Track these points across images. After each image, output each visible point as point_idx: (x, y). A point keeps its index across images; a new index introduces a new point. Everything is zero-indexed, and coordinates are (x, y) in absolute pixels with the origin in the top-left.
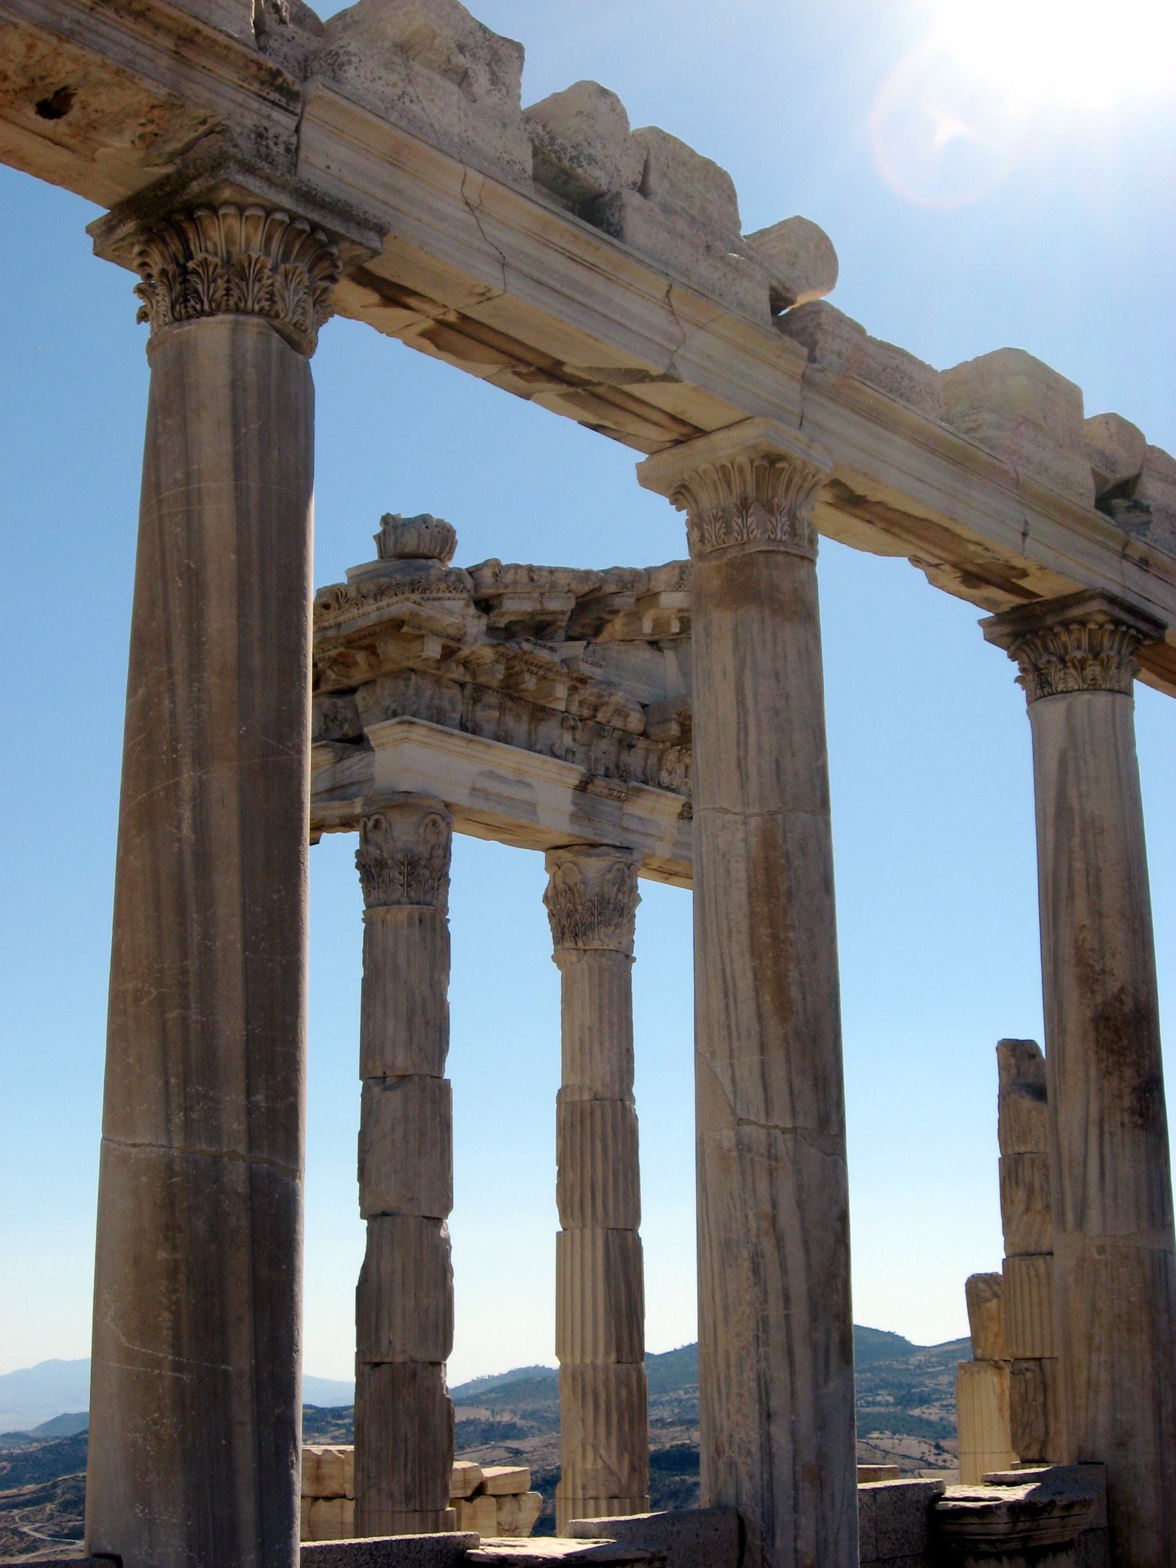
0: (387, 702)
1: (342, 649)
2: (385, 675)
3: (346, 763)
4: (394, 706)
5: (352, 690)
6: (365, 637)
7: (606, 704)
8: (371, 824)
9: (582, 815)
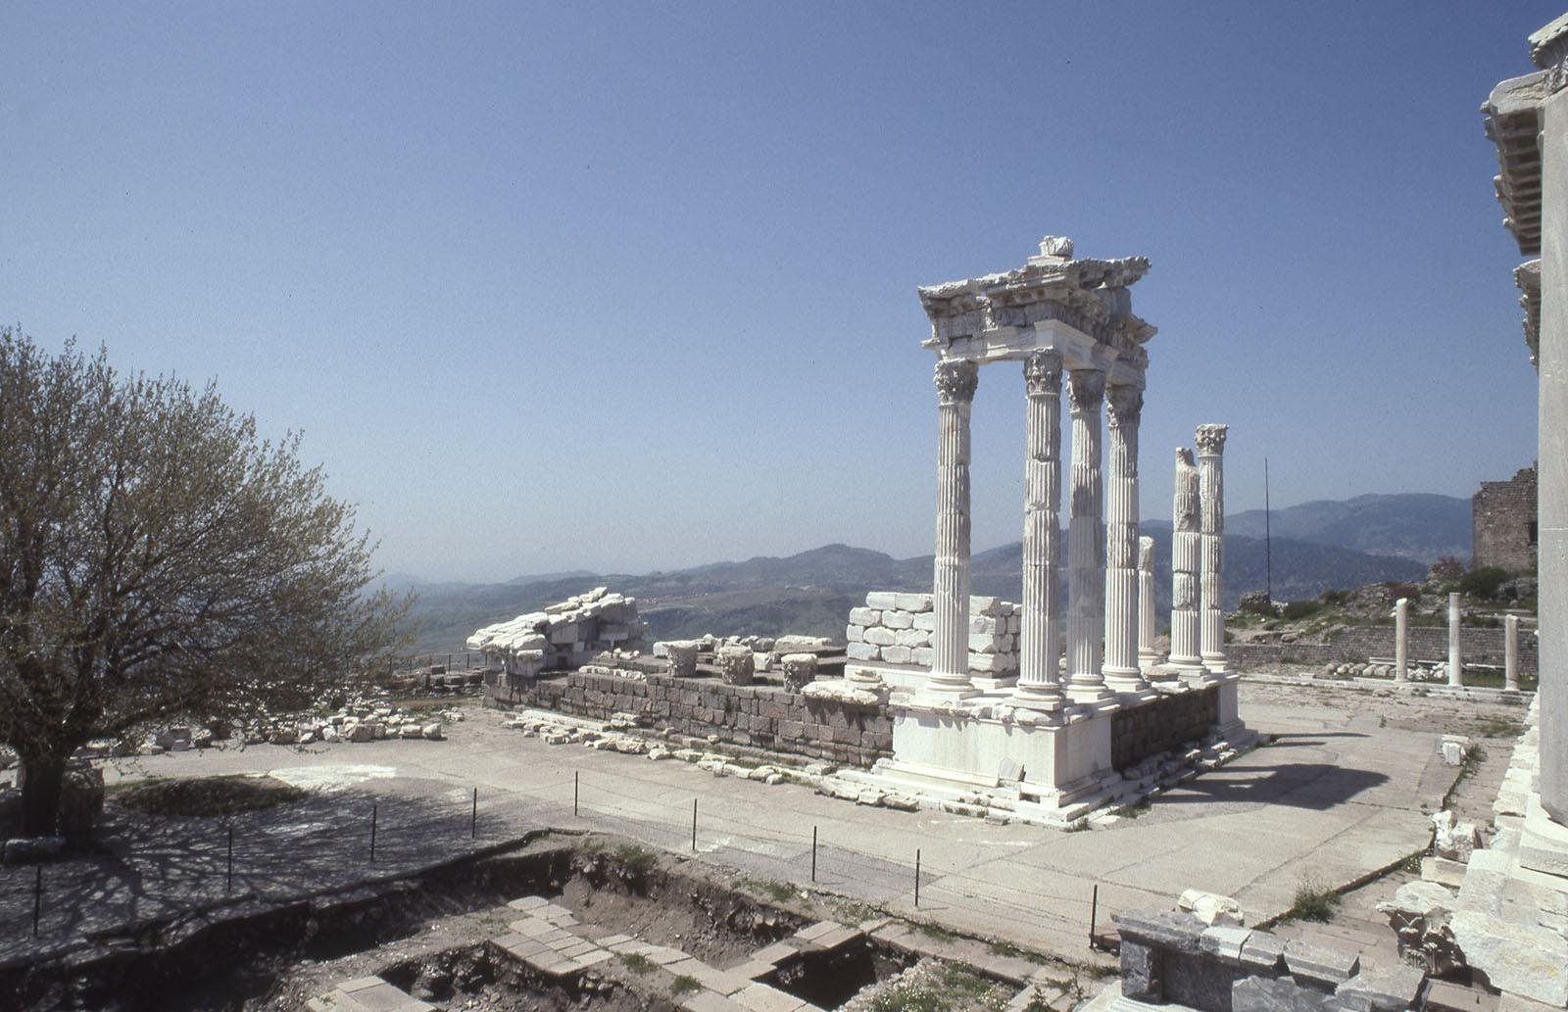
2: (1041, 301)
5: (1023, 306)
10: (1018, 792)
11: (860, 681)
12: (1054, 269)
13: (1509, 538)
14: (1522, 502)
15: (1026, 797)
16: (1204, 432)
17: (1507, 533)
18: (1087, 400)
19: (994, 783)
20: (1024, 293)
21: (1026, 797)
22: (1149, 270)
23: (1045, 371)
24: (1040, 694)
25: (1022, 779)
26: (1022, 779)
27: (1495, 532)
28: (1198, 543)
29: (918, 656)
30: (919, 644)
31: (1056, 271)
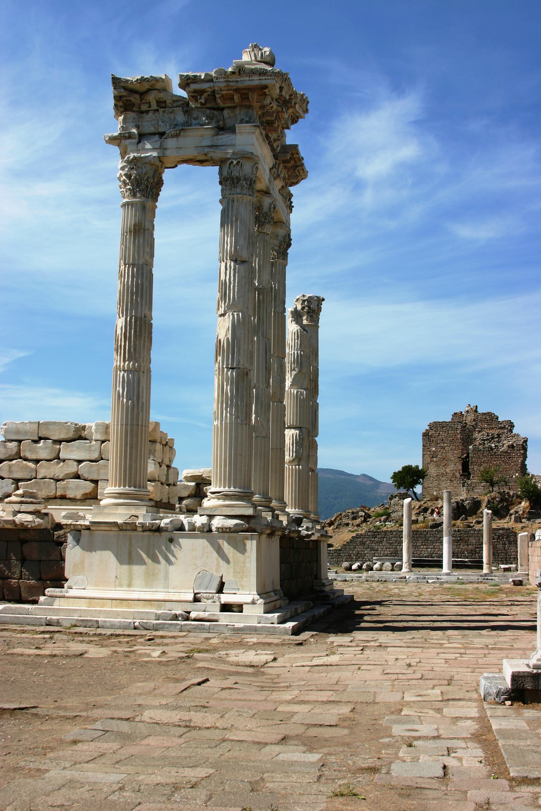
0: (243, 117)
1: (231, 92)
3: (220, 137)
4: (247, 119)
6: (245, 89)
7: (279, 140)
8: (235, 162)
10: (218, 603)
11: (21, 503)
13: (447, 470)
14: (457, 439)
15: (226, 608)
19: (191, 597)
21: (226, 608)
24: (231, 500)
25: (220, 590)
26: (220, 590)
27: (438, 466)
29: (65, 488)
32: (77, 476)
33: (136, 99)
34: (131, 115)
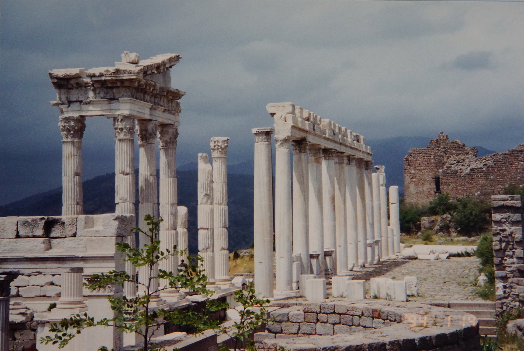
9: (151, 115)
12: (130, 73)
14: (431, 163)
16: (215, 142)
17: (423, 184)
18: (146, 137)
20: (113, 82)
22: (180, 60)
23: (125, 125)
27: (417, 185)
28: (212, 211)
30: (47, 284)
31: (131, 73)
32: (52, 284)
33: (65, 83)
34: (63, 91)
